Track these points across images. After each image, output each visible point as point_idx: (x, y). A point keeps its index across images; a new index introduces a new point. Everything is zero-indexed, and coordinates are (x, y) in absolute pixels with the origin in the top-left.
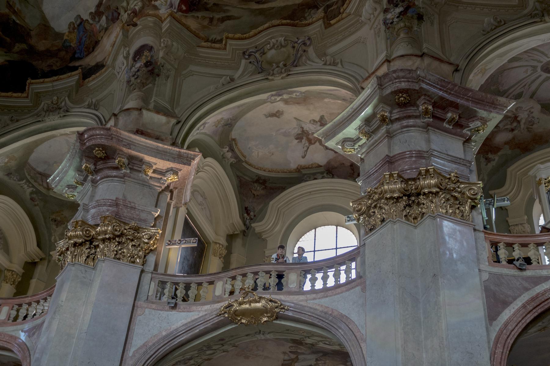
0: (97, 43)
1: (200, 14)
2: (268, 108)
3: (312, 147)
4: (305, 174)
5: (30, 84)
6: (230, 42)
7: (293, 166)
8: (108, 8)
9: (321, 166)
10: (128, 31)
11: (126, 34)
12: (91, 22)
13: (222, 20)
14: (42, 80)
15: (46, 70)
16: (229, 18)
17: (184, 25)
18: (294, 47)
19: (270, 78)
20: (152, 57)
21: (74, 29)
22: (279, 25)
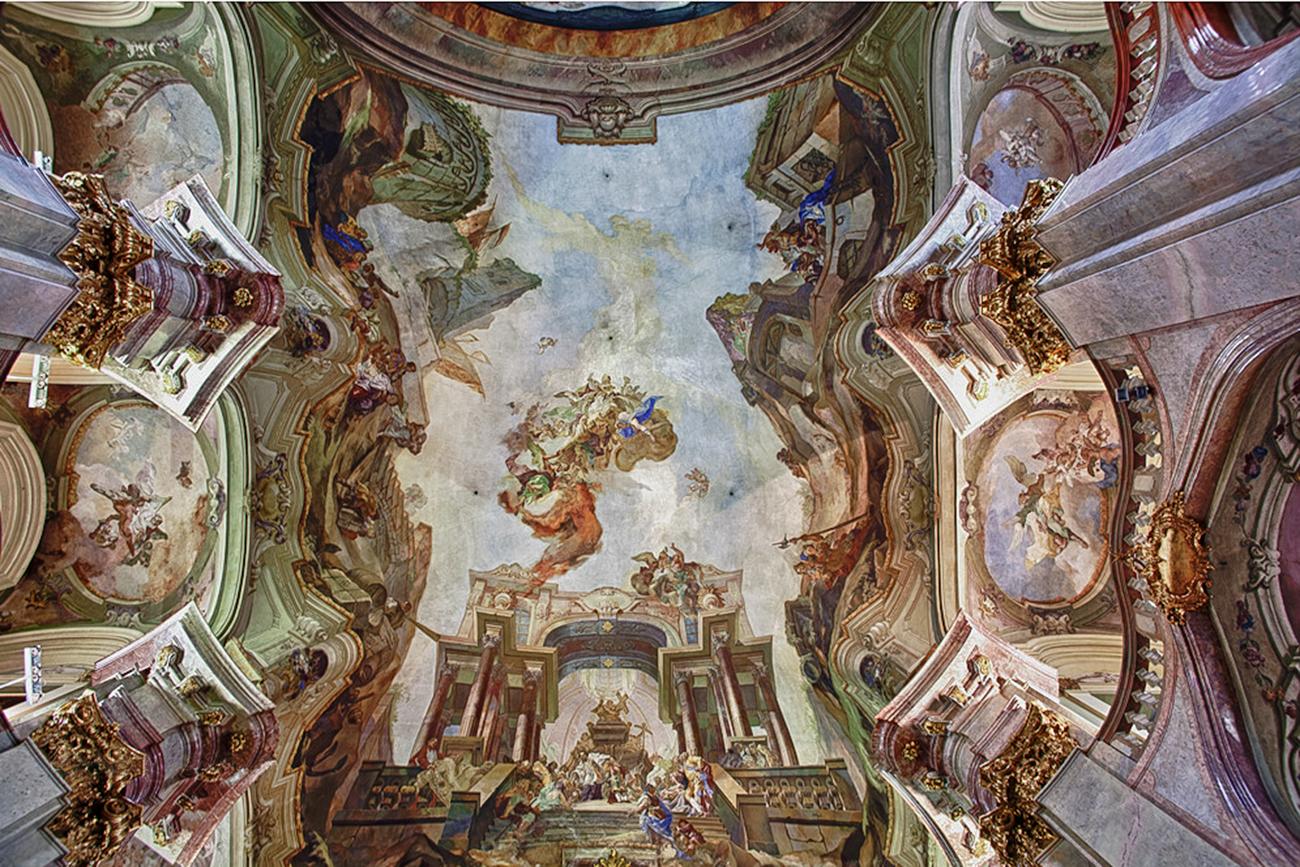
0: (338, 264)
1: (342, 409)
2: (199, 470)
3: (110, 504)
4: (58, 481)
5: (308, 148)
6: (302, 438)
7: (79, 468)
8: (376, 295)
9: (69, 508)
10: (348, 317)
11: (346, 313)
12: (363, 263)
13: (328, 433)
14: (308, 166)
15: (319, 178)
16: (328, 441)
17: (338, 389)
18: (276, 520)
19: (249, 491)
20: (316, 347)
21: (359, 235)
22: (305, 499)
